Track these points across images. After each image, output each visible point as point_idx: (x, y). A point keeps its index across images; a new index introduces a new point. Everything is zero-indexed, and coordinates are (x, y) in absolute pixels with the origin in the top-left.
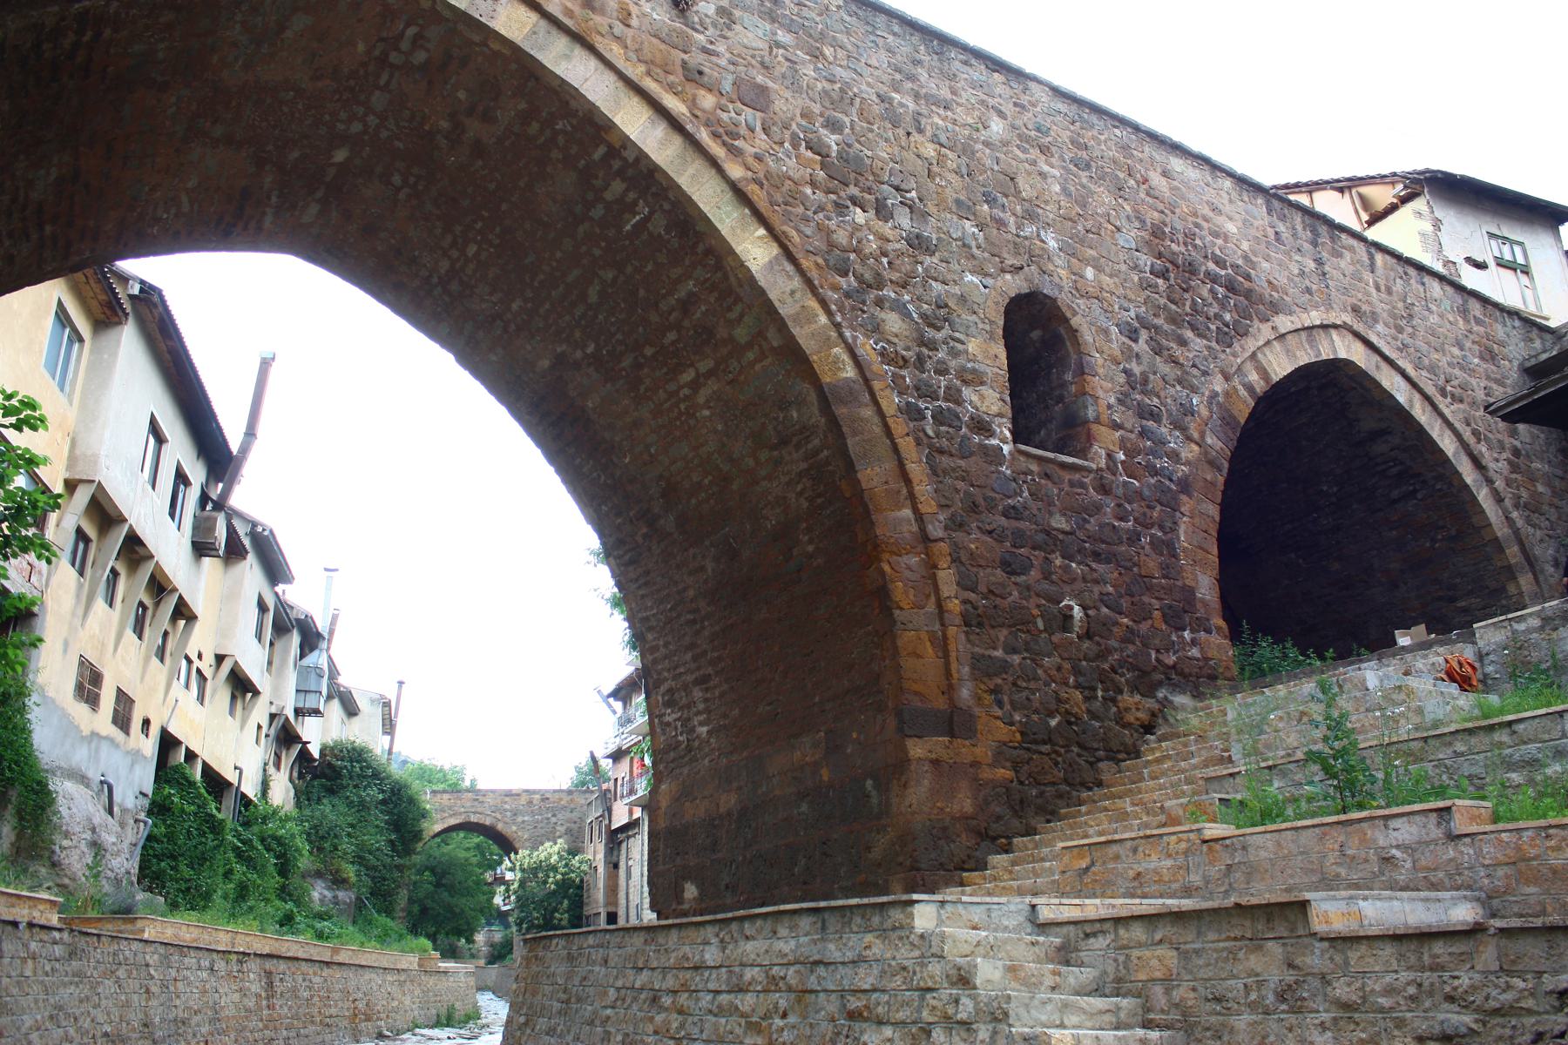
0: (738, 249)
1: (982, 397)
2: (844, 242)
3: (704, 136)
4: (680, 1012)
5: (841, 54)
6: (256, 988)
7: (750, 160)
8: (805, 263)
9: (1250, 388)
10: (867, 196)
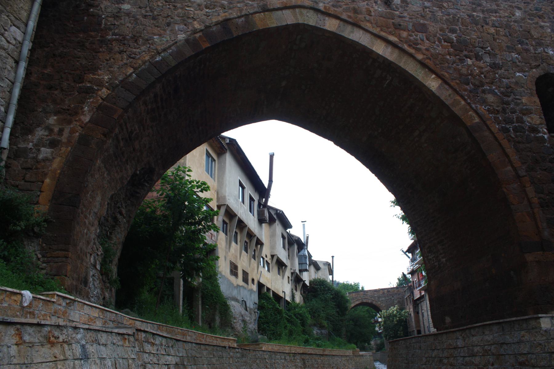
0: (427, 84)
1: (532, 119)
2: (465, 73)
3: (406, 47)
4: (451, 365)
5: (450, 4)
6: (300, 364)
7: (424, 51)
8: (452, 84)
10: (471, 54)
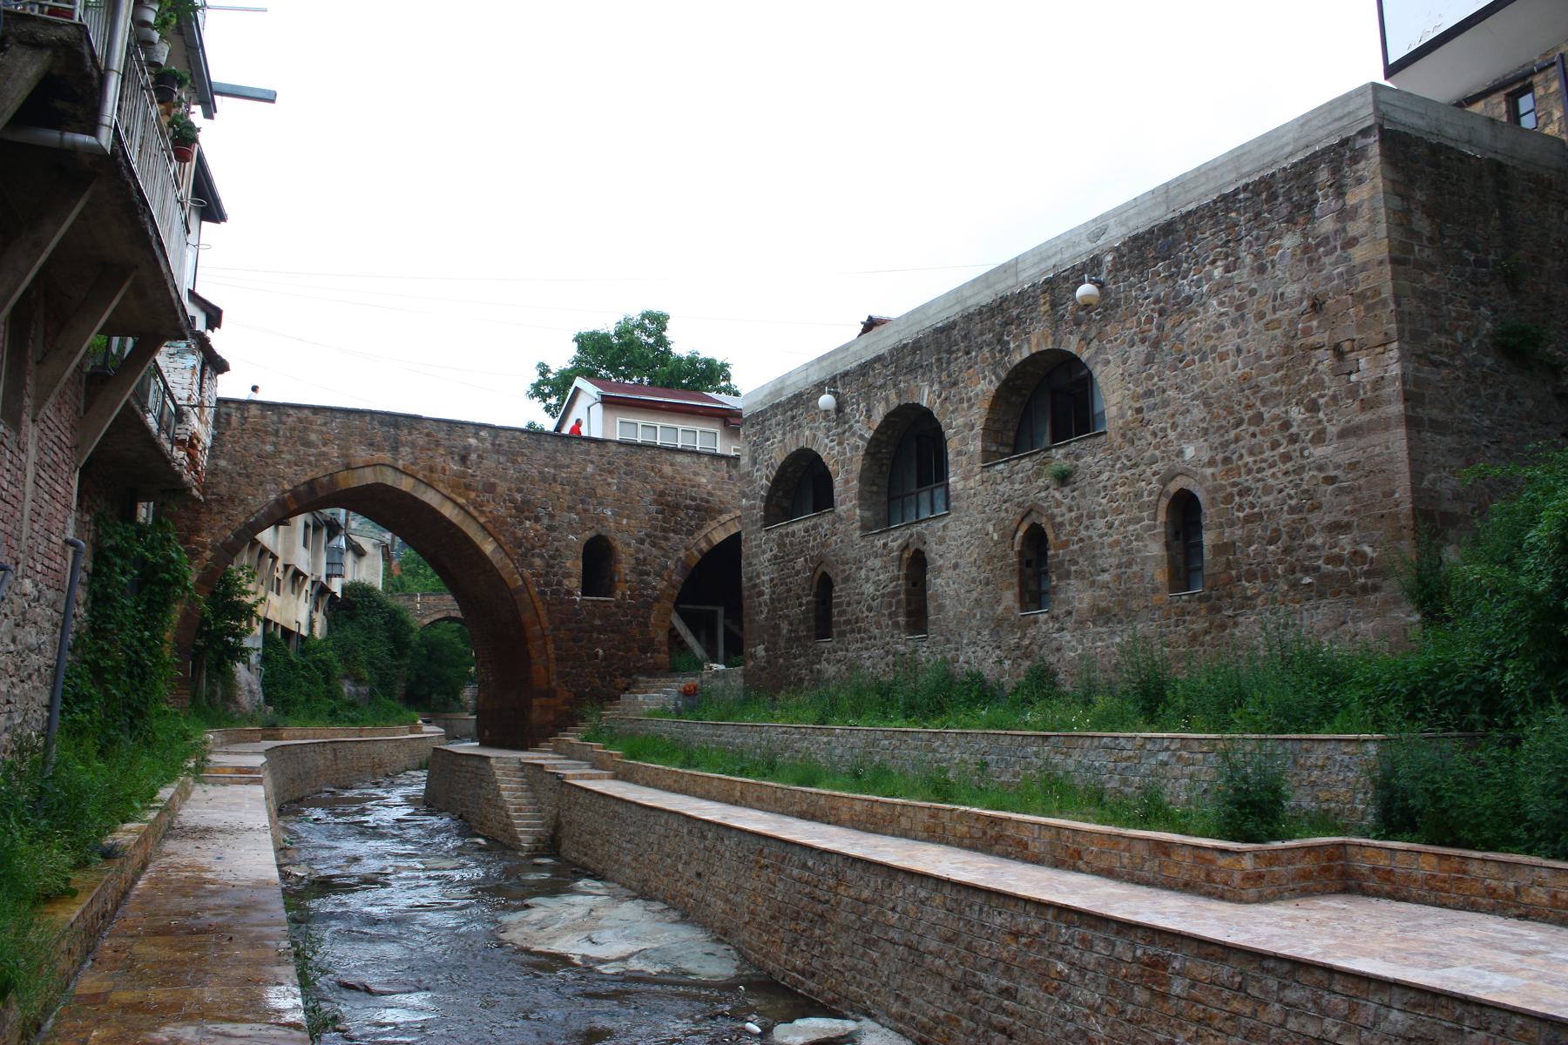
9: (700, 551)
